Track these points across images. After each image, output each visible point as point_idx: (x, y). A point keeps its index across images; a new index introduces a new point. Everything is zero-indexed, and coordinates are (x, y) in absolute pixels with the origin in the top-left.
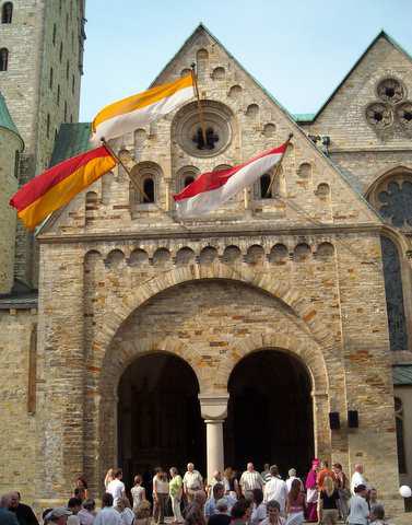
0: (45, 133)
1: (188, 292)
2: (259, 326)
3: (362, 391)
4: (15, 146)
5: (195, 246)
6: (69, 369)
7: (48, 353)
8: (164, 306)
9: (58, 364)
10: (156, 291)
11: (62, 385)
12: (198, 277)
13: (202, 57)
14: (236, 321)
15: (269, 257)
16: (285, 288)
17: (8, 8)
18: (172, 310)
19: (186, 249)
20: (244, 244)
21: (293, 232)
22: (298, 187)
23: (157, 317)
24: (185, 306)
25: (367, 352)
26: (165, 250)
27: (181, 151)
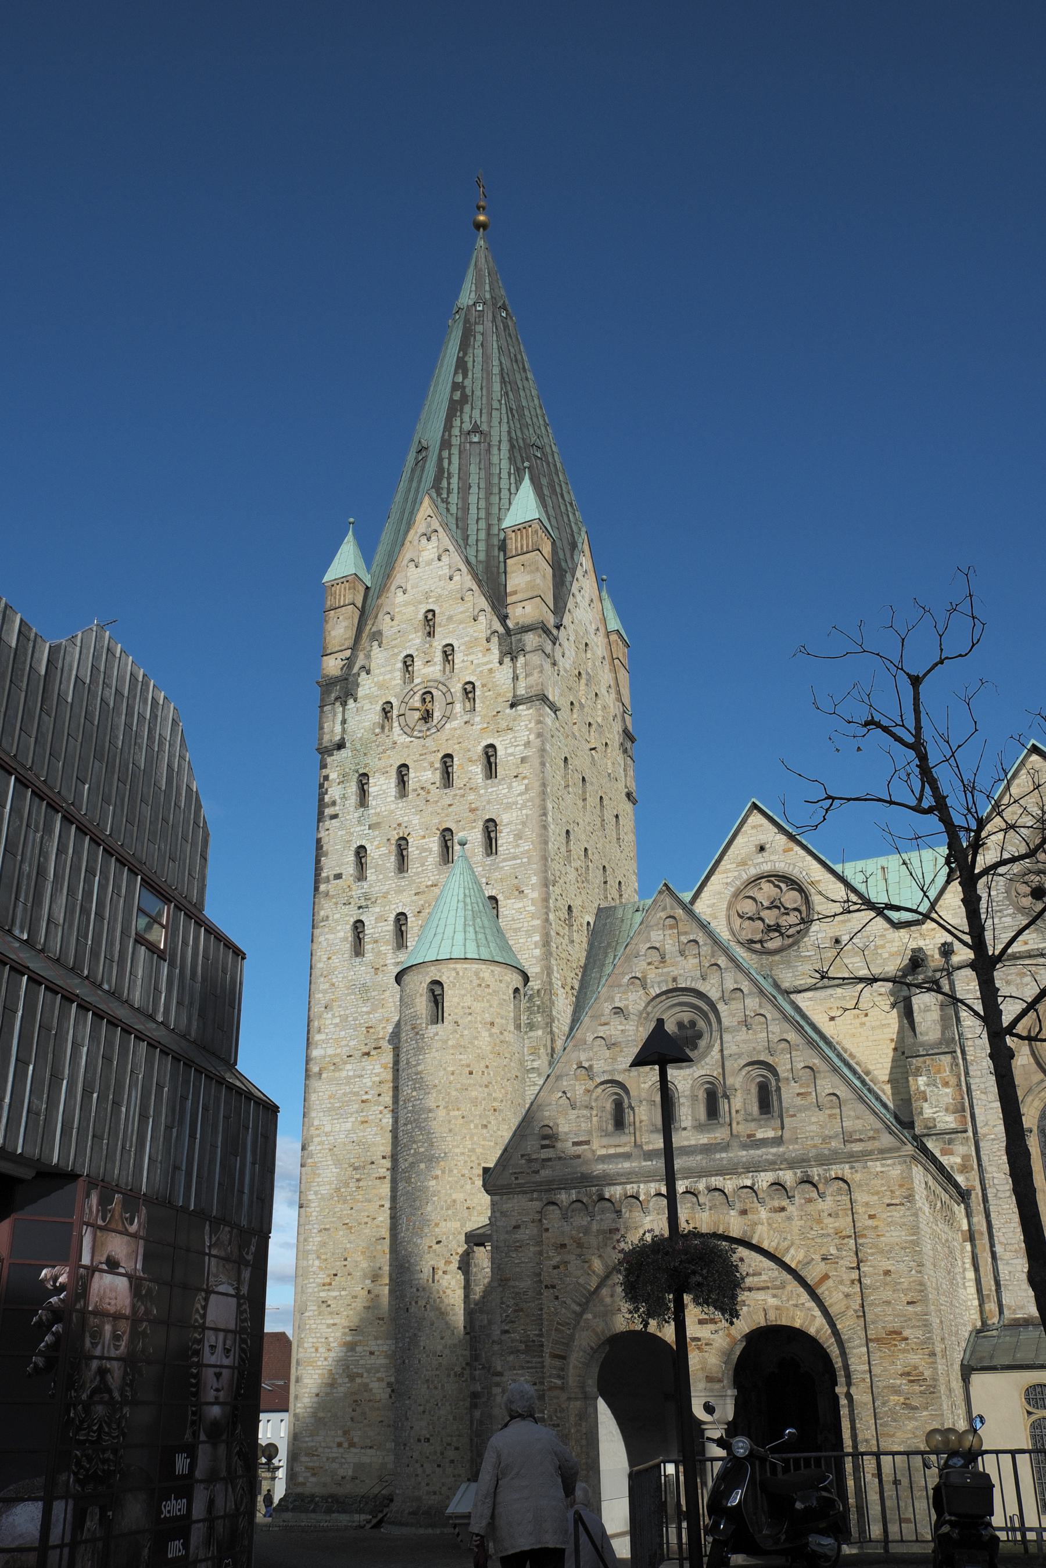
3: (896, 1390)
13: (671, 927)
16: (786, 1244)
17: (491, 751)
20: (729, 1184)
25: (901, 1333)
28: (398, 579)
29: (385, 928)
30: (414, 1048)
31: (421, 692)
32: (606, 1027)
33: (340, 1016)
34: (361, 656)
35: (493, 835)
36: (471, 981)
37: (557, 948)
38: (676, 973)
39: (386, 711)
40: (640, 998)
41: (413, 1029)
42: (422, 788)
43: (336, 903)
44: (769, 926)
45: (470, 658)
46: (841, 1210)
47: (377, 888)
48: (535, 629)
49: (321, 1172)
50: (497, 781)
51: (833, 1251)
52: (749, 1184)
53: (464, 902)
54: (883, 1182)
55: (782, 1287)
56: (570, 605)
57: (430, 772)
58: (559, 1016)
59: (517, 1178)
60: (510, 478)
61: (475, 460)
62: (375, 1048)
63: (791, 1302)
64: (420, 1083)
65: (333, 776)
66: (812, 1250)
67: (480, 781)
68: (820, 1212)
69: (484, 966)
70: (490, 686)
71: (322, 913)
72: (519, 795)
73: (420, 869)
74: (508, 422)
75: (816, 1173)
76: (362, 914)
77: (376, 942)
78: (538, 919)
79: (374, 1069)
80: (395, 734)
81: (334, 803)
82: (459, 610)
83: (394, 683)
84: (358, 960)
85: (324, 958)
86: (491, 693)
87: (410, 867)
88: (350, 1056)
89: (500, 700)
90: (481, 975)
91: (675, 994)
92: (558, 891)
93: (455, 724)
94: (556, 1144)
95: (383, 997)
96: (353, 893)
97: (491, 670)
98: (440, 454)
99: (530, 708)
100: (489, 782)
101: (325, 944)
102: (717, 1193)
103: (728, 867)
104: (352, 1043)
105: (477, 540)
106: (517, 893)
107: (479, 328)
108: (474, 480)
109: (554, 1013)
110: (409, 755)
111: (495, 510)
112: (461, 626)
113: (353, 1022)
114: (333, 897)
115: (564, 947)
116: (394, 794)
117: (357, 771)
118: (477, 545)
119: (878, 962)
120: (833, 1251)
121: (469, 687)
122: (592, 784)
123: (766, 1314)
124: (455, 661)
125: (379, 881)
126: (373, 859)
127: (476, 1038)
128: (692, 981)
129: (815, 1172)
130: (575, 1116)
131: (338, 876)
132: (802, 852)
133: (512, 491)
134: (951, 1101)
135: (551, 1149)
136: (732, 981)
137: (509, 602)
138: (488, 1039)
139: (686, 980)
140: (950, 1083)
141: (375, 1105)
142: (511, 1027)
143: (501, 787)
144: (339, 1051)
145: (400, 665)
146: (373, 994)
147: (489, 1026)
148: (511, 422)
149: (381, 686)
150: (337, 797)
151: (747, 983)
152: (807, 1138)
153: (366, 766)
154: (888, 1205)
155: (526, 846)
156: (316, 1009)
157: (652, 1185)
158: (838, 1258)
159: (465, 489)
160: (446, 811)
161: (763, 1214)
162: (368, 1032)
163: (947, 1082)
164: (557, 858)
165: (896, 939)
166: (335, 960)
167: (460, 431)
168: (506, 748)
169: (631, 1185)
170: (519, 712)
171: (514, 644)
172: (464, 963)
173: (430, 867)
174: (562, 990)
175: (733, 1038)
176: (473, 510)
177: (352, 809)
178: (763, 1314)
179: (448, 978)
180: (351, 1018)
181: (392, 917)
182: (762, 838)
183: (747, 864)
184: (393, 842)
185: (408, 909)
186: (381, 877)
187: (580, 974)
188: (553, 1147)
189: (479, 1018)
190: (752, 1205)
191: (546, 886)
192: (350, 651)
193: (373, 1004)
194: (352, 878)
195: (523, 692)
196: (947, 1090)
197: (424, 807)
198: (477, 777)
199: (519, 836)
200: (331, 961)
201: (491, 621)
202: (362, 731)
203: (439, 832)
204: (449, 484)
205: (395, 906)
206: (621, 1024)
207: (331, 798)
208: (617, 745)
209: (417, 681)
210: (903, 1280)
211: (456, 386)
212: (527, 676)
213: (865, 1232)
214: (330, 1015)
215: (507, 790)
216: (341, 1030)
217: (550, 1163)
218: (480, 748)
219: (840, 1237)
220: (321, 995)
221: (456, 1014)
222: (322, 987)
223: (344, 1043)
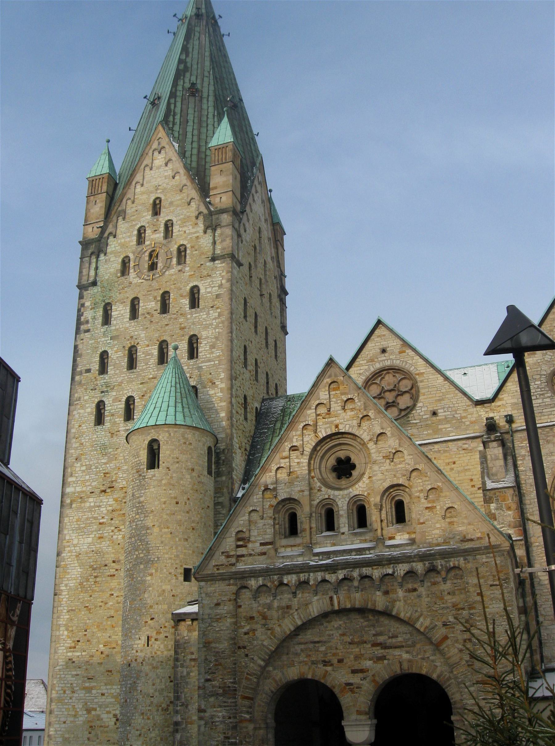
0: (242, 418)
1: (329, 622)
2: (397, 652)
4: (210, 442)
5: (332, 578)
6: (225, 700)
7: (207, 684)
8: (309, 635)
9: (217, 695)
10: (299, 623)
11: (220, 714)
12: (336, 607)
13: (334, 389)
14: (374, 648)
15: (401, 586)
18: (317, 639)
19: (324, 581)
20: (376, 573)
21: (422, 557)
22: (427, 513)
23: (303, 646)
24: (329, 635)
26: (306, 582)
27: (319, 484)
28: (138, 177)
29: (119, 406)
30: (138, 486)
31: (150, 251)
32: (287, 460)
33: (86, 465)
34: (110, 226)
35: (195, 345)
36: (179, 440)
37: (237, 421)
38: (338, 422)
39: (125, 263)
40: (311, 439)
41: (137, 472)
42: (148, 313)
43: (86, 389)
44: (388, 403)
45: (184, 229)
46: (458, 590)
47: (115, 379)
48: (228, 212)
50: (199, 309)
51: (451, 619)
52: (390, 573)
53: (176, 387)
54: (487, 569)
55: (413, 645)
56: (250, 200)
57: (154, 303)
58: (237, 468)
59: (218, 569)
60: (214, 118)
61: (191, 105)
62: (110, 488)
63: (419, 657)
64: (141, 509)
65: (87, 304)
66: (436, 619)
67: (188, 309)
68: (442, 592)
69: (188, 430)
70: (196, 247)
71: (76, 395)
72: (215, 319)
73: (145, 367)
74: (214, 85)
75: (439, 564)
76: (103, 396)
77: (113, 415)
78: (225, 401)
80: (131, 277)
81: (87, 322)
82: (177, 198)
83: (131, 244)
84: (100, 427)
86: (197, 252)
87: (138, 365)
88: (93, 492)
89: (203, 257)
90: (186, 436)
91: (336, 437)
92: (239, 385)
93: (172, 271)
94: (248, 544)
95: (116, 452)
96: (98, 382)
97: (197, 237)
98: (169, 100)
99: (224, 263)
100: (193, 310)
101: (77, 416)
102: (366, 580)
103: (361, 362)
104: (94, 484)
105: (191, 155)
106: (210, 384)
107: (197, 29)
108: (191, 117)
109: (234, 465)
110: (139, 292)
111: (203, 137)
112: (178, 209)
114: (84, 385)
115: (241, 422)
116: (128, 316)
117: (104, 301)
118: (191, 157)
119: (462, 427)
120: (451, 619)
121: (182, 248)
122: (261, 317)
123: (401, 665)
124: (174, 231)
125: (116, 374)
126: (113, 359)
127: (181, 479)
128: (349, 428)
129: (439, 563)
130: (261, 525)
131: (88, 371)
132: (412, 353)
133: (215, 126)
134: (513, 520)
135: (244, 549)
136: (379, 428)
137: (211, 194)
138: (190, 480)
139: (345, 427)
140: (512, 507)
141: (109, 526)
142: (206, 473)
143: (202, 314)
144: (84, 489)
145: (136, 232)
146: (110, 450)
147: (190, 471)
148: (216, 85)
149: (122, 245)
150: (89, 318)
151: (390, 429)
152: (432, 539)
153: (110, 297)
154: (491, 586)
155: (217, 353)
156: (70, 460)
157: (319, 573)
158: (454, 624)
159: (184, 122)
160: (163, 329)
161: (401, 593)
162: (105, 476)
163: (510, 507)
164: (238, 361)
165: (475, 412)
166: (84, 427)
167: (183, 88)
168: (206, 288)
169: (304, 574)
170: (216, 265)
171: (214, 221)
172: (175, 428)
173: (151, 366)
174: (239, 450)
175: (380, 467)
176: (189, 135)
177: (100, 326)
178: (399, 665)
179: (163, 437)
180: (94, 467)
181: (124, 399)
182: (384, 344)
183: (374, 361)
184: (127, 348)
185: (135, 394)
186: (118, 371)
187: (251, 441)
188: (246, 546)
189: (184, 465)
190: (393, 588)
191: (231, 380)
192: (103, 222)
193: (109, 457)
194: (97, 372)
195: (219, 252)
196: (510, 513)
197: (149, 326)
198: (186, 306)
199: (213, 347)
200: (81, 428)
201: (199, 205)
202: (109, 275)
203: (158, 343)
204: (174, 119)
205: (126, 391)
206: (297, 457)
207: (85, 318)
208: (276, 294)
209: (147, 243)
210: (501, 638)
211: (180, 61)
212: (222, 241)
213: (474, 605)
214: (79, 465)
215: (205, 316)
216: (86, 475)
217: (243, 559)
218: (188, 288)
219: (456, 609)
220: (73, 451)
221: (168, 462)
222: (74, 445)
223: (88, 484)
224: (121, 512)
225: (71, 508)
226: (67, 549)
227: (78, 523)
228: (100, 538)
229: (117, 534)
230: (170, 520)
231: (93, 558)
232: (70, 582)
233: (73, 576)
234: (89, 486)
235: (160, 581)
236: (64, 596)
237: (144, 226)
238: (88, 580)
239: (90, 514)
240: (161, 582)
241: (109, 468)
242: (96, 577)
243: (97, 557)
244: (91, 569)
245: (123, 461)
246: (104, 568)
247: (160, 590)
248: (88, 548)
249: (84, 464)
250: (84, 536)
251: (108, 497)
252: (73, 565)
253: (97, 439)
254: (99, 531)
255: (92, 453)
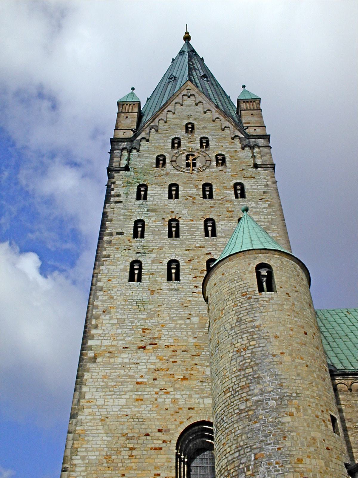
43: (117, 249)
47: (154, 244)
49: (91, 439)
79: (149, 359)
85: (105, 280)
95: (158, 309)
113: (130, 324)
141: (150, 387)
144: (115, 343)
146: (149, 307)
166: (114, 282)
173: (197, 237)
181: (166, 261)
186: (157, 237)
200: (110, 282)
216: (117, 329)
224: (168, 372)
225: (95, 362)
226: (87, 411)
227: (105, 380)
228: (137, 400)
229: (163, 396)
230: (302, 350)
231: (127, 424)
232: (89, 454)
233: (94, 446)
234: (121, 340)
235: (305, 424)
236: (79, 473)
237: (179, 139)
238: (118, 452)
239: (123, 371)
240: (308, 426)
241: (149, 324)
242: (131, 449)
243: (135, 423)
244: (124, 438)
245: (168, 318)
246: (145, 438)
247: (309, 438)
248: (119, 410)
249: (114, 317)
250: (114, 397)
251: (149, 354)
252: (96, 431)
253: (131, 294)
254: (137, 391)
255: (126, 307)
